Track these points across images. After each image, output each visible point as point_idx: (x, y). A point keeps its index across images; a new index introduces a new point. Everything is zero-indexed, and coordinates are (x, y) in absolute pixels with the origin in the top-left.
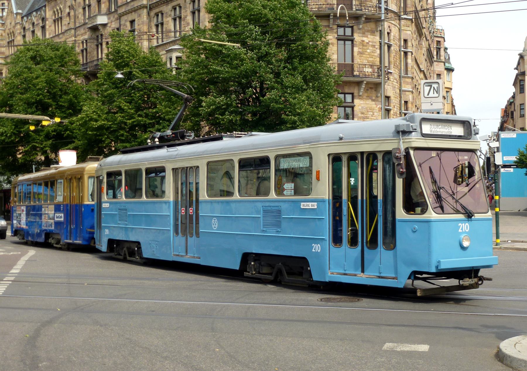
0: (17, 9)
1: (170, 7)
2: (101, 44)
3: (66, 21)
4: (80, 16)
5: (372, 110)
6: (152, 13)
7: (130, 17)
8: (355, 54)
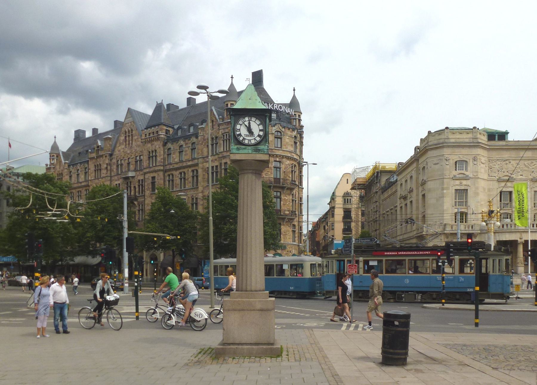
0: (65, 160)
1: (178, 172)
2: (130, 187)
3: (104, 171)
4: (114, 170)
5: (288, 231)
6: (166, 174)
7: (152, 175)
8: (282, 205)
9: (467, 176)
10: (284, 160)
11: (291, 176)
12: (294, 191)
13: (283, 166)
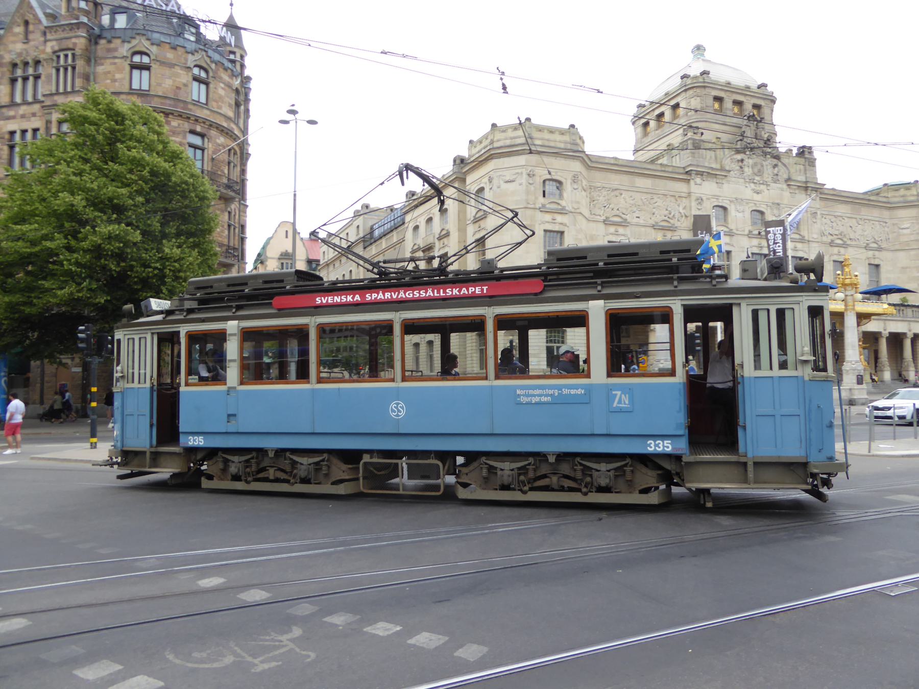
9: (564, 208)
10: (213, 133)
11: (226, 171)
12: (233, 206)
13: (209, 146)
